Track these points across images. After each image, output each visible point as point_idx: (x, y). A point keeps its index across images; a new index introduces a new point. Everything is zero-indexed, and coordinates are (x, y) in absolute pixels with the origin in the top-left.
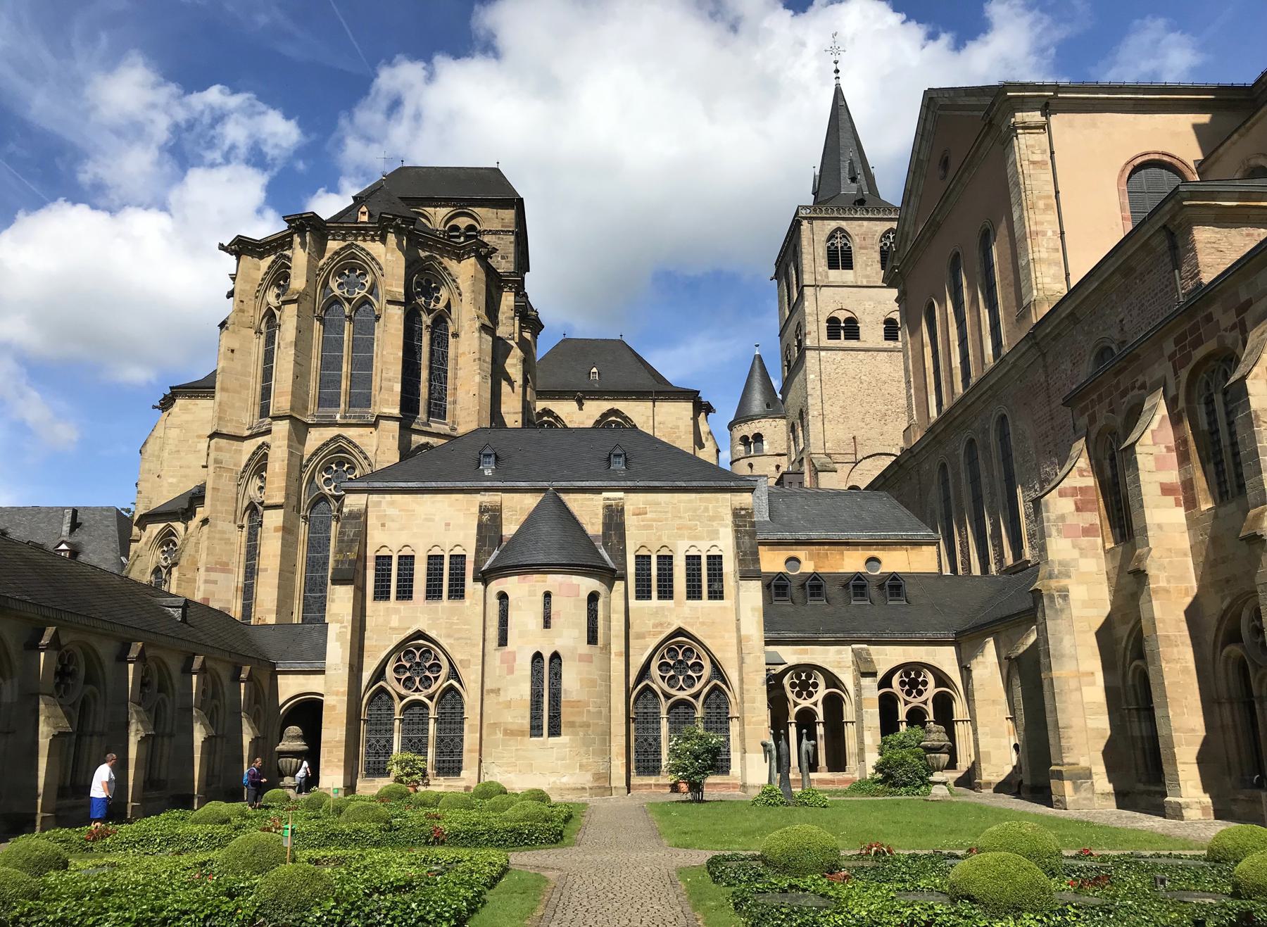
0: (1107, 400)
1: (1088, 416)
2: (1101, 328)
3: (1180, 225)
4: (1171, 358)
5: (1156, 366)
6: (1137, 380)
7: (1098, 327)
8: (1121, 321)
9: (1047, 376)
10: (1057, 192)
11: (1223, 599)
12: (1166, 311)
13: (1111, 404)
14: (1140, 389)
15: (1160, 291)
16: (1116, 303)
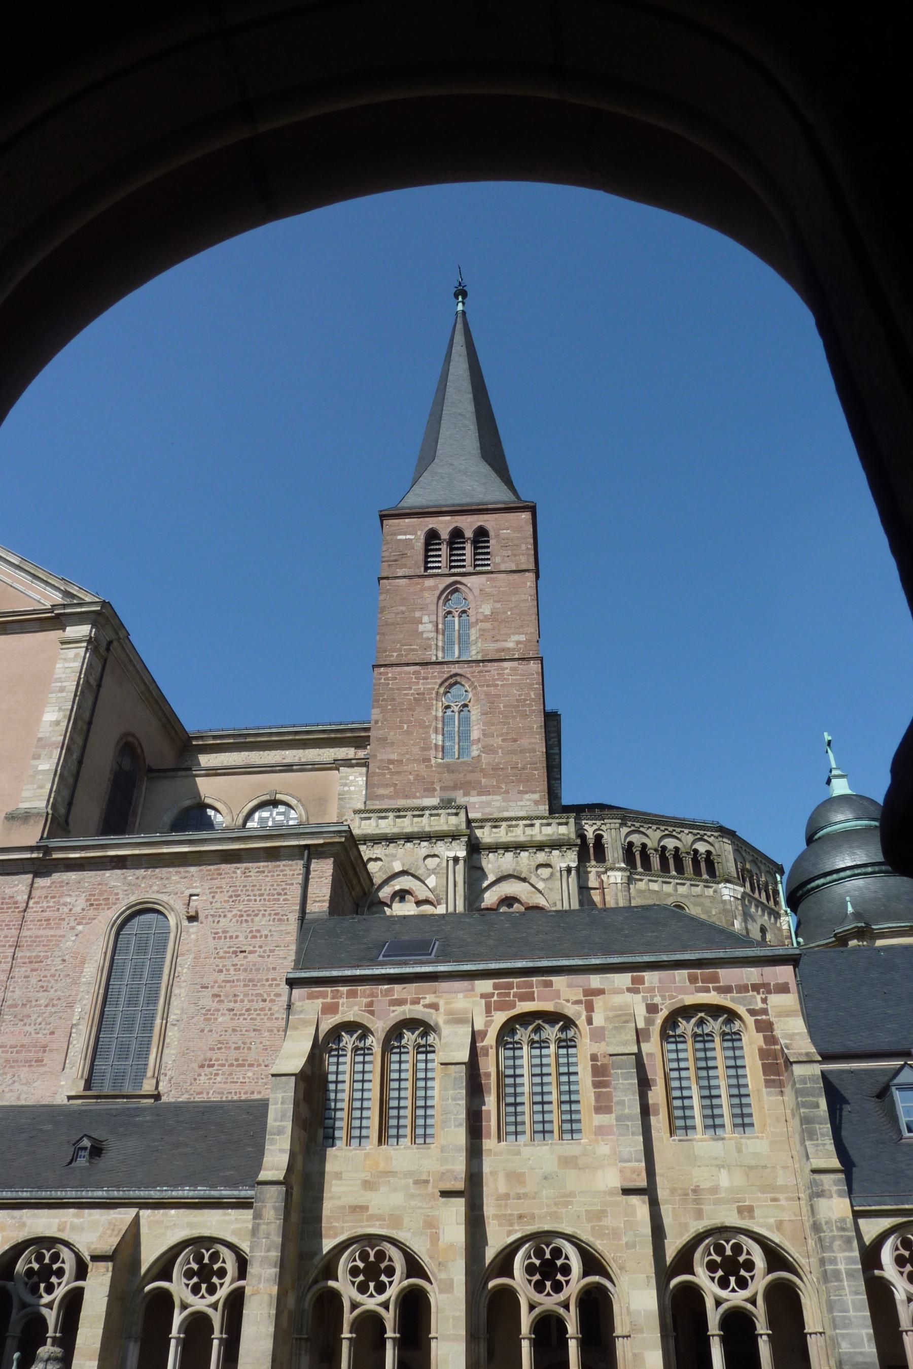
0: (365, 1000)
1: (323, 1003)
2: (155, 888)
3: (324, 852)
4: (483, 996)
5: (461, 996)
6: (425, 998)
7: (151, 886)
8: (191, 895)
9: (29, 897)
10: (90, 723)
11: (509, 1233)
12: (270, 915)
13: (370, 1004)
14: (425, 1006)
15: (269, 895)
16: (193, 876)
